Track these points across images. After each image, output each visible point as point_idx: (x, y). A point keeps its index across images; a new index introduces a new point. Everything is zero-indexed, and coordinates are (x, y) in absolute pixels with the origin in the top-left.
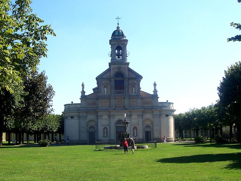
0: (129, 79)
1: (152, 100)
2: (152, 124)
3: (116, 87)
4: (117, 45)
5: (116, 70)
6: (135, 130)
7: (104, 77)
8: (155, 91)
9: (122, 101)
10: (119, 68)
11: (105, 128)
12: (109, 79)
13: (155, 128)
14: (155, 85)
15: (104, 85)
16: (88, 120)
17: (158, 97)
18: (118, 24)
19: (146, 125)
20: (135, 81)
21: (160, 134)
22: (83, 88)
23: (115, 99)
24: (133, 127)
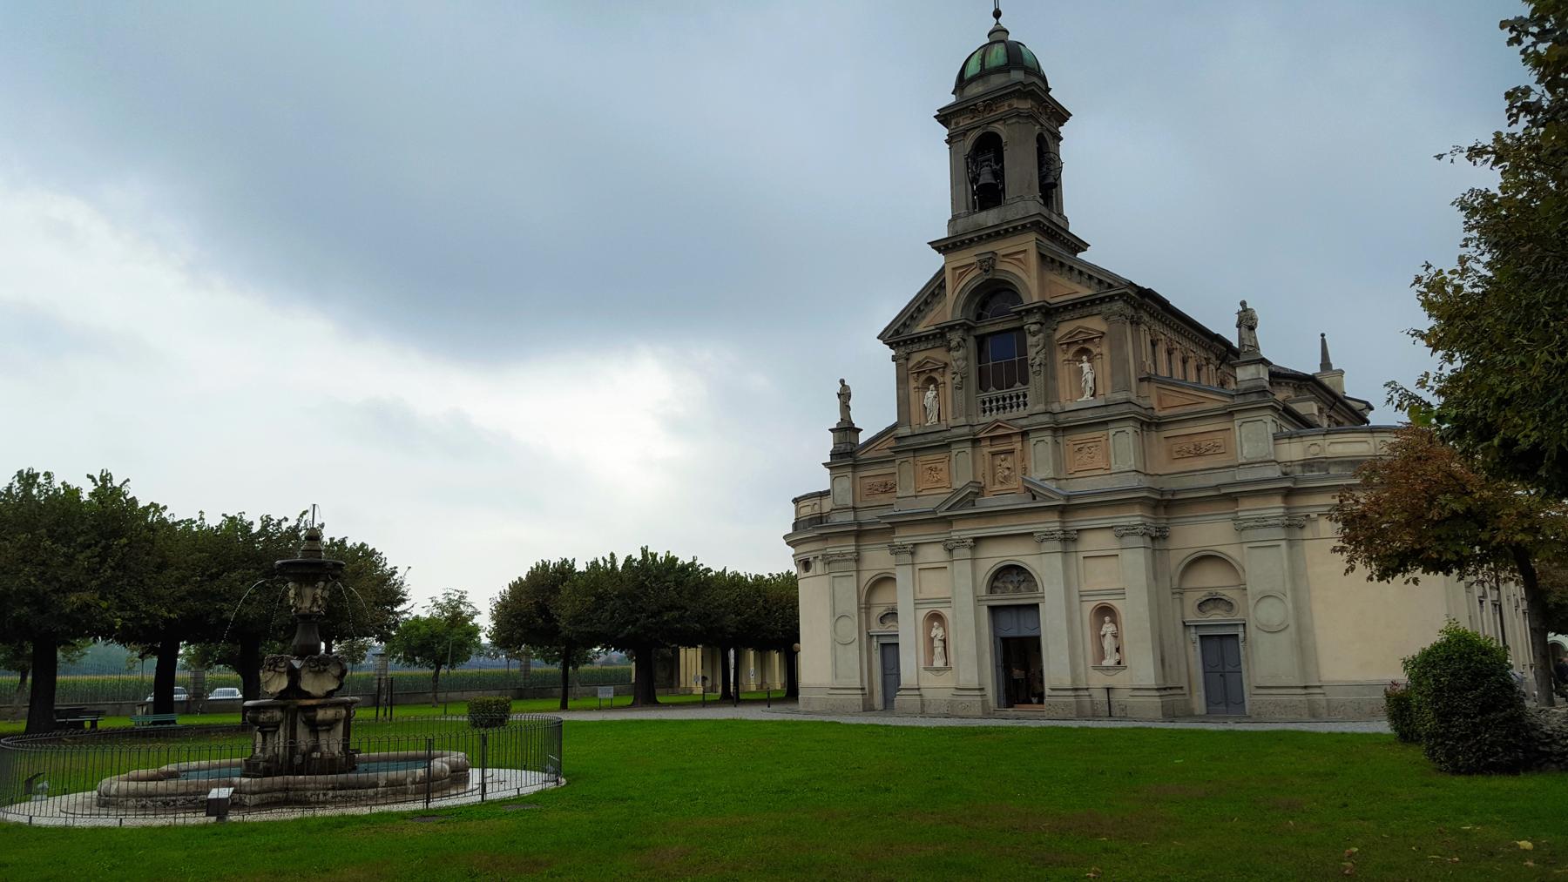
0: (1050, 313)
1: (1228, 425)
2: (1242, 588)
3: (981, 373)
4: (973, 136)
5: (973, 277)
7: (921, 328)
9: (1011, 452)
10: (988, 263)
11: (936, 617)
12: (940, 335)
13: (1270, 613)
15: (923, 377)
16: (867, 576)
18: (997, 14)
19: (1201, 596)
21: (1304, 648)
22: (845, 408)
23: (976, 442)
24: (1089, 607)
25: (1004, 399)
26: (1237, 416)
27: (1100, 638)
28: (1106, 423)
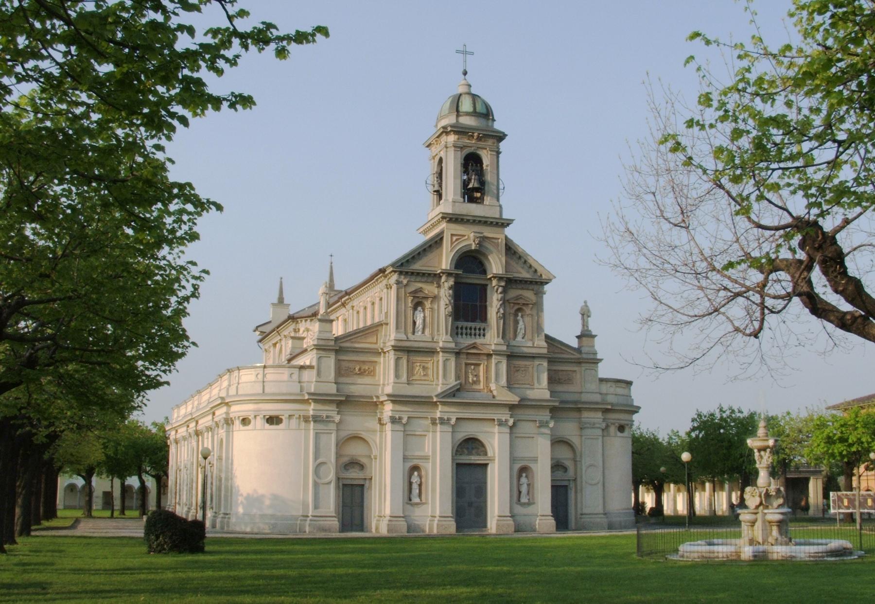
6: (524, 480)
8: (586, 335)
14: (585, 314)
17: (599, 357)
20: (529, 295)
25: (471, 329)
26: (583, 365)
27: (519, 485)
28: (534, 357)
